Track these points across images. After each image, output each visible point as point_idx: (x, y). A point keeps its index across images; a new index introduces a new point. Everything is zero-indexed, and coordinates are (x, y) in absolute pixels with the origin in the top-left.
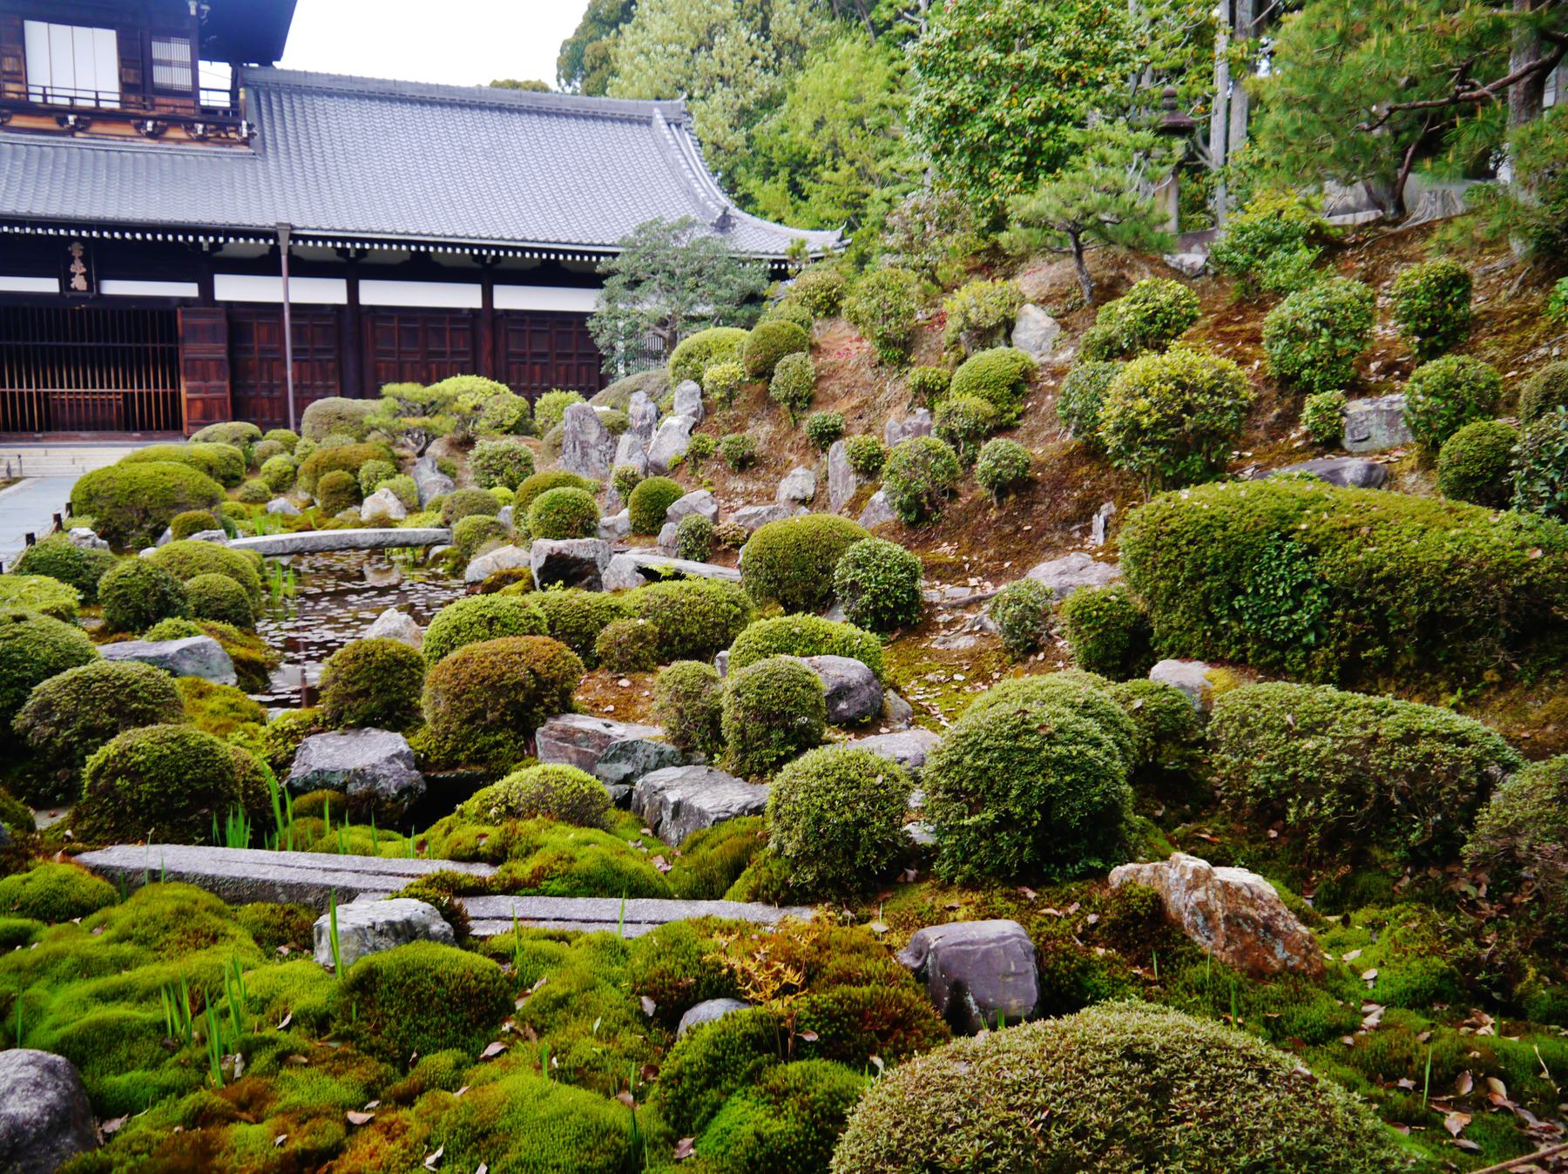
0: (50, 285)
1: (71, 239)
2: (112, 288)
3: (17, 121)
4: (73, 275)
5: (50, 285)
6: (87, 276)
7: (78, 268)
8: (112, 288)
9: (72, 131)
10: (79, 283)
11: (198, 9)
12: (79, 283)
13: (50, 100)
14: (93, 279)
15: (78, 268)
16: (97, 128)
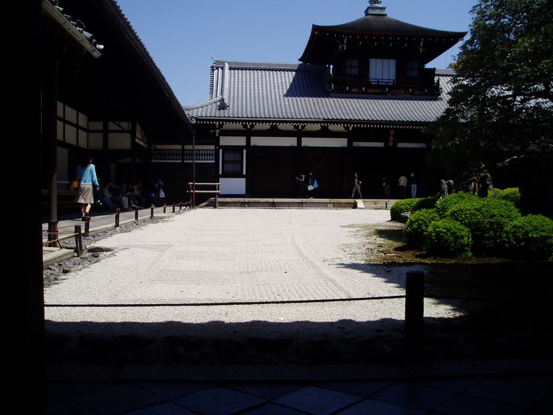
0: (381, 145)
1: (390, 129)
2: (401, 145)
3: (370, 91)
4: (389, 141)
5: (381, 145)
6: (393, 141)
7: (391, 138)
8: (401, 145)
9: (386, 93)
10: (391, 144)
11: (422, 51)
12: (391, 144)
13: (380, 83)
14: (395, 143)
15: (391, 138)
16: (394, 91)
